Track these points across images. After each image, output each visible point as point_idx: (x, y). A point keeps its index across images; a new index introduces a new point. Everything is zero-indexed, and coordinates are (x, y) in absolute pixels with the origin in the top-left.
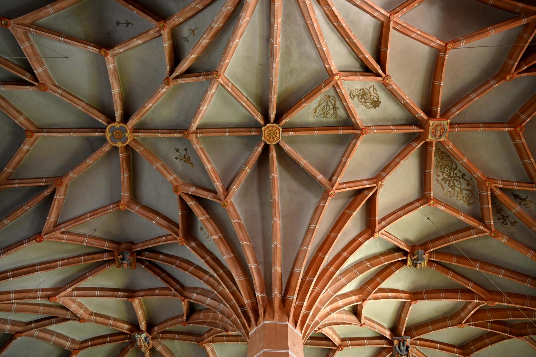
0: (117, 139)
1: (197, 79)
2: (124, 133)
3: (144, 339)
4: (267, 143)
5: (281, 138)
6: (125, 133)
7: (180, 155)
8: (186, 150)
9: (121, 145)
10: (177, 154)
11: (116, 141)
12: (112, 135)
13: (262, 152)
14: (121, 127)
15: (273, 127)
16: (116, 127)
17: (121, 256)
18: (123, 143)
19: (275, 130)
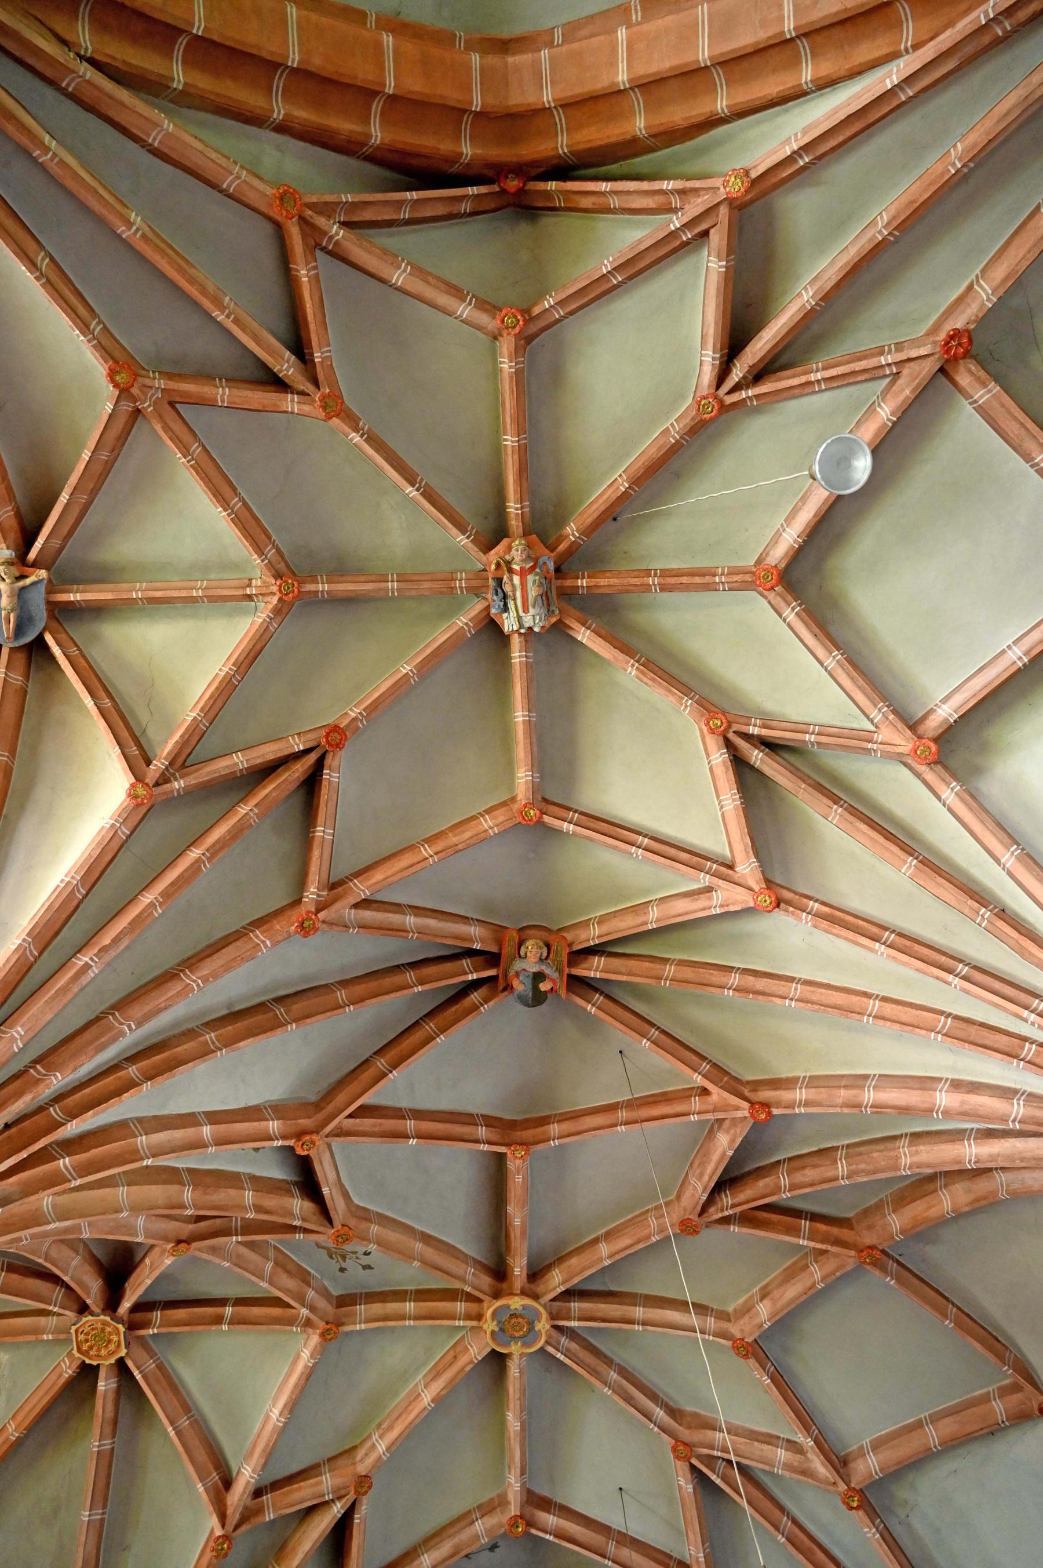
0: (521, 1316)
1: (280, 1512)
2: (501, 1329)
3: (511, 604)
4: (108, 1319)
5: (73, 1331)
6: (496, 1329)
7: (358, 1261)
8: (342, 1270)
9: (510, 1302)
10: (365, 1260)
11: (523, 1309)
12: (531, 1324)
13: (124, 1283)
14: (507, 1345)
15: (98, 1356)
16: (519, 1344)
17: (544, 987)
18: (508, 1307)
19: (91, 1348)
